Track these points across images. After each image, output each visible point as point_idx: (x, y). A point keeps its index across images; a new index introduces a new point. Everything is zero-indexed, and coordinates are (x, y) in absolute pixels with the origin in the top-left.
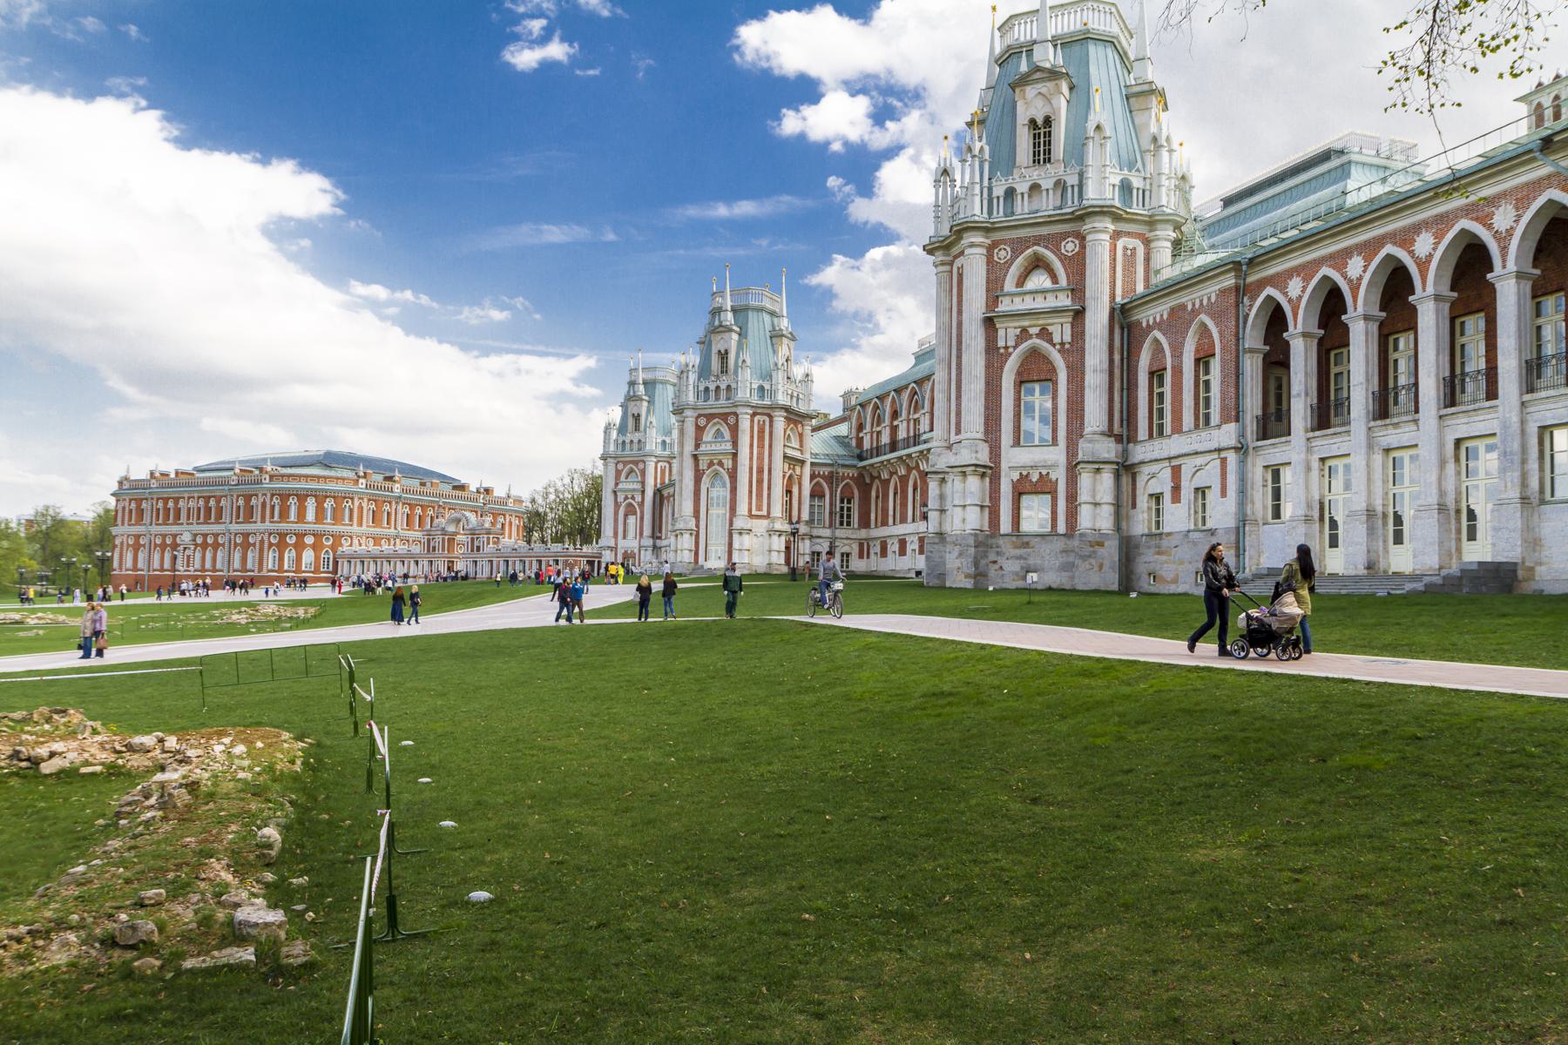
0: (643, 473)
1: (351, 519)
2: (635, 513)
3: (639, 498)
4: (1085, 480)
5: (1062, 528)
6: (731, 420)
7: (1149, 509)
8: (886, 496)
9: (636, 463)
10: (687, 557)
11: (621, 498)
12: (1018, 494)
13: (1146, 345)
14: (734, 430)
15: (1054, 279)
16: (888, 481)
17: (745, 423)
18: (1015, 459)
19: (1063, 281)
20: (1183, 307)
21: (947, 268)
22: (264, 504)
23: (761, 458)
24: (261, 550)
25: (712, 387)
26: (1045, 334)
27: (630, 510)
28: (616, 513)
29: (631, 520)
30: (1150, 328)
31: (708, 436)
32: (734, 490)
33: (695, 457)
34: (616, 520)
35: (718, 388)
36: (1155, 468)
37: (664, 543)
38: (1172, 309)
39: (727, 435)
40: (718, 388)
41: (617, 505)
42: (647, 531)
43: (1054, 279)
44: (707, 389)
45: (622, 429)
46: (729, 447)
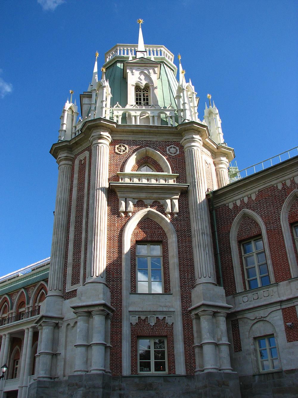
4: (205, 324)
5: (181, 369)
7: (255, 350)
12: (136, 336)
13: (236, 219)
20: (273, 188)
21: (70, 163)
30: (237, 209)
36: (262, 313)
38: (260, 191)
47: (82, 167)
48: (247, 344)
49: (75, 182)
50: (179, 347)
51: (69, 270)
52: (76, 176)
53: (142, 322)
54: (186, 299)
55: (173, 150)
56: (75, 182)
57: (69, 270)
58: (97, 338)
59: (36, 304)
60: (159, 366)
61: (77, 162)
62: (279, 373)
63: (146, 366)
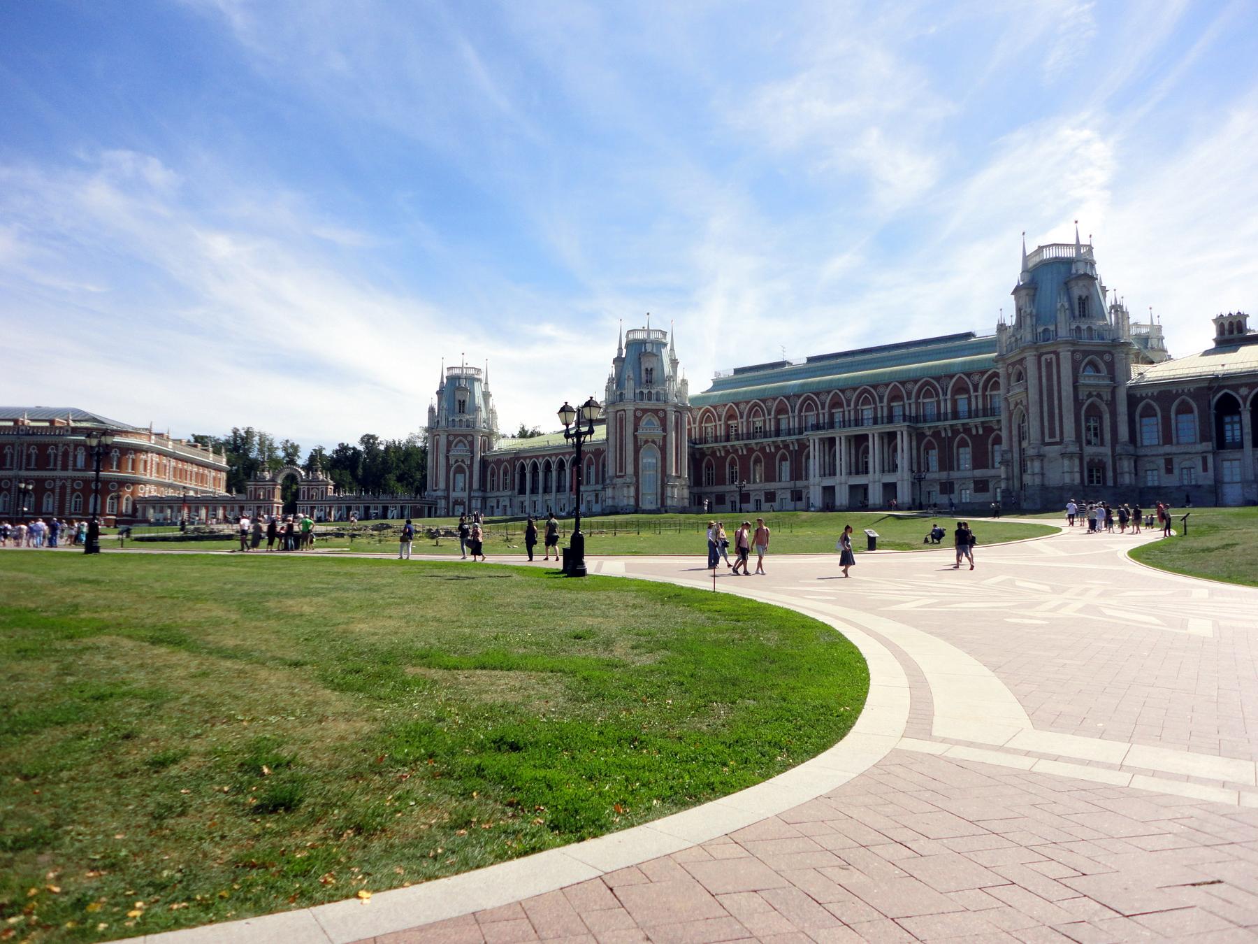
0: (472, 444)
5: (1110, 483)
6: (661, 414)
8: (721, 466)
9: (465, 436)
10: (632, 502)
11: (452, 461)
14: (663, 422)
15: (1098, 371)
16: (726, 458)
18: (1089, 450)
19: (1104, 371)
20: (1170, 392)
22: (66, 454)
25: (645, 391)
26: (1099, 396)
27: (460, 470)
29: (460, 478)
30: (1142, 398)
31: (643, 423)
32: (664, 459)
33: (635, 437)
35: (650, 393)
40: (650, 393)
41: (448, 466)
42: (476, 485)
43: (1098, 371)
44: (642, 393)
45: (451, 411)
46: (659, 432)
47: (1049, 364)
48: (1141, 473)
49: (1044, 374)
50: (1110, 474)
51: (1047, 431)
52: (1044, 369)
53: (1091, 461)
54: (1113, 450)
55: (1107, 357)
56: (1044, 374)
57: (1047, 431)
58: (1077, 469)
60: (1098, 482)
61: (1043, 359)
62: (1159, 487)
63: (1092, 482)
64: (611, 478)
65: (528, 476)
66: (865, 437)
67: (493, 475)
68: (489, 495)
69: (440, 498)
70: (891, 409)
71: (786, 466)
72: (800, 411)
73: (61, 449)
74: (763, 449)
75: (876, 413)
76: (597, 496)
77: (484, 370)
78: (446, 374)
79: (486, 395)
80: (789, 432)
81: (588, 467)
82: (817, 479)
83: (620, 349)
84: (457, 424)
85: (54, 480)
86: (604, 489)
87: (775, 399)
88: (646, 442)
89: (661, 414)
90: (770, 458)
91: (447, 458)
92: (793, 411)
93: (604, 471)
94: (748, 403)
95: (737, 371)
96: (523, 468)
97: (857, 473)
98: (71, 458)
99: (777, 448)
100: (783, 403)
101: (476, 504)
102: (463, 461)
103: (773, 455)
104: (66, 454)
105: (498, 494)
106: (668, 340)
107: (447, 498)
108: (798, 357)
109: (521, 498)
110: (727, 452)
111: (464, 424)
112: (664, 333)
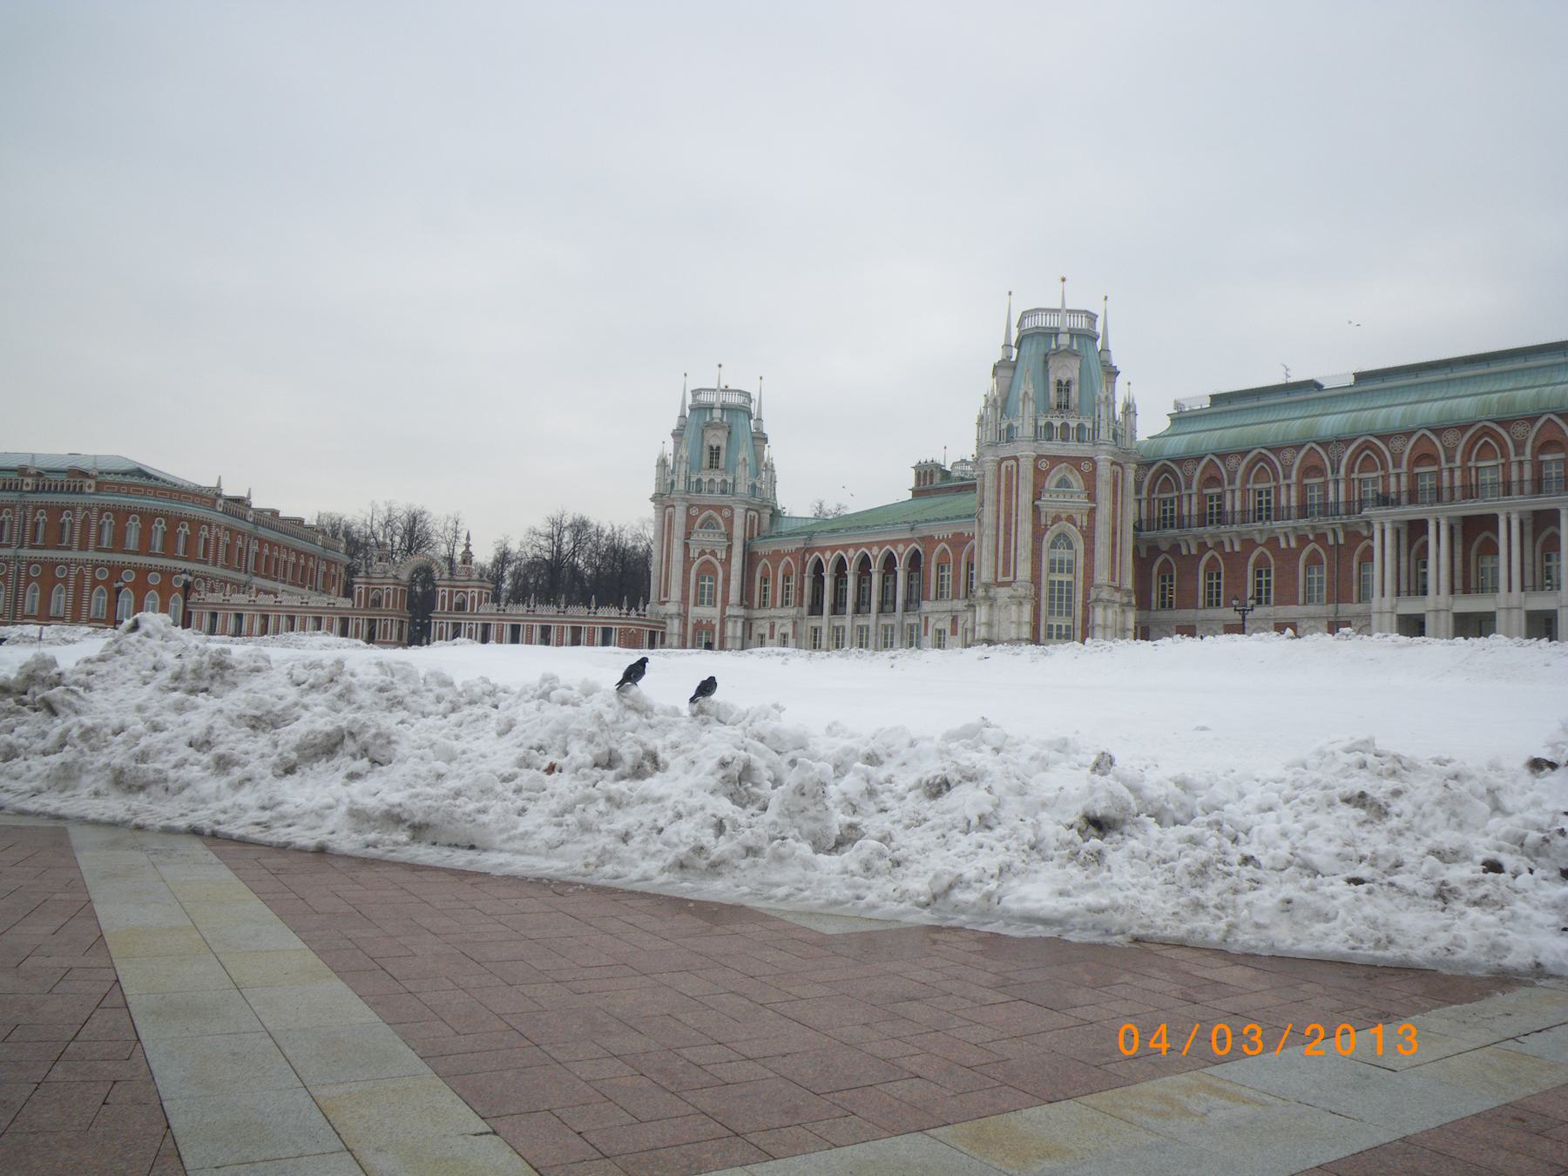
0: (730, 522)
1: (206, 553)
2: (715, 573)
3: (722, 555)
6: (1086, 467)
9: (719, 509)
11: (694, 553)
14: (1090, 480)
16: (1199, 557)
17: (1104, 472)
22: (86, 523)
23: (1114, 517)
24: (79, 589)
25: (1057, 423)
28: (686, 572)
31: (1051, 483)
32: (1090, 552)
33: (1036, 510)
34: (686, 580)
35: (1065, 426)
37: (757, 613)
39: (1077, 483)
42: (734, 596)
44: (1049, 426)
45: (693, 465)
46: (1083, 499)
59: (1470, 464)
64: (987, 587)
65: (828, 583)
66: (1490, 522)
67: (765, 580)
68: (757, 613)
69: (671, 617)
70: (1538, 466)
71: (1321, 575)
72: (1350, 469)
73: (80, 516)
74: (1273, 542)
75: (1507, 474)
76: (954, 620)
77: (755, 396)
78: (689, 401)
79: (760, 438)
80: (1326, 509)
81: (940, 568)
82: (1389, 600)
83: (1007, 346)
84: (705, 487)
85: (67, 565)
86: (972, 607)
87: (1299, 447)
88: (1057, 519)
89: (1086, 467)
90: (1290, 556)
91: (686, 546)
92: (1336, 470)
93: (969, 577)
94: (1244, 454)
95: (1216, 399)
96: (819, 567)
97: (1466, 590)
98: (93, 531)
99: (1303, 540)
100: (1315, 456)
101: (734, 629)
102: (713, 553)
103: (1292, 555)
104: (86, 523)
105: (773, 612)
106: (1099, 329)
107: (683, 617)
108: (1335, 371)
109: (815, 621)
110: (1203, 547)
111: (717, 489)
112: (1092, 318)
